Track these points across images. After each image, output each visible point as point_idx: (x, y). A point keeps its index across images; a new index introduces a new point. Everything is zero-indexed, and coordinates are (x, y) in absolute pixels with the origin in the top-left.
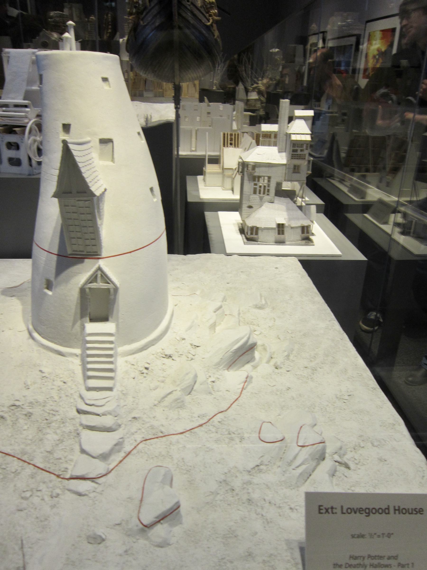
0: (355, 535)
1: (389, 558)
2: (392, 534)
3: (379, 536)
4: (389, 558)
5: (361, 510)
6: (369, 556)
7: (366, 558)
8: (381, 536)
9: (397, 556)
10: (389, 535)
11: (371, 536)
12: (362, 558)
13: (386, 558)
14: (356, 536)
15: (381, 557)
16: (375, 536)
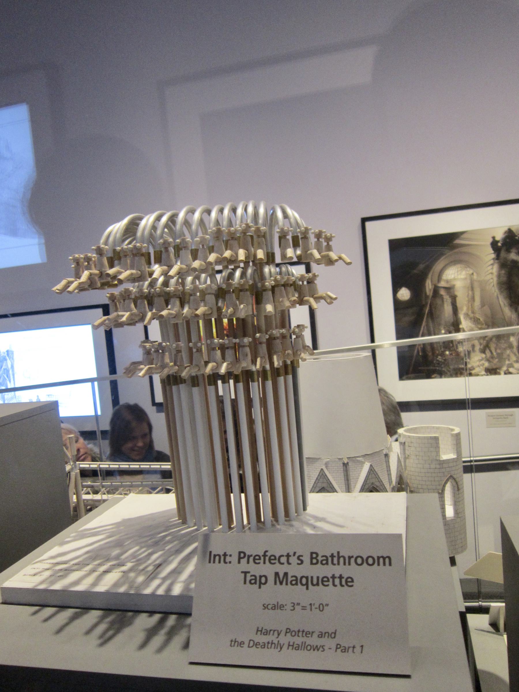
4: (321, 635)
6: (288, 631)
12: (276, 633)
13: (315, 635)
15: (308, 634)
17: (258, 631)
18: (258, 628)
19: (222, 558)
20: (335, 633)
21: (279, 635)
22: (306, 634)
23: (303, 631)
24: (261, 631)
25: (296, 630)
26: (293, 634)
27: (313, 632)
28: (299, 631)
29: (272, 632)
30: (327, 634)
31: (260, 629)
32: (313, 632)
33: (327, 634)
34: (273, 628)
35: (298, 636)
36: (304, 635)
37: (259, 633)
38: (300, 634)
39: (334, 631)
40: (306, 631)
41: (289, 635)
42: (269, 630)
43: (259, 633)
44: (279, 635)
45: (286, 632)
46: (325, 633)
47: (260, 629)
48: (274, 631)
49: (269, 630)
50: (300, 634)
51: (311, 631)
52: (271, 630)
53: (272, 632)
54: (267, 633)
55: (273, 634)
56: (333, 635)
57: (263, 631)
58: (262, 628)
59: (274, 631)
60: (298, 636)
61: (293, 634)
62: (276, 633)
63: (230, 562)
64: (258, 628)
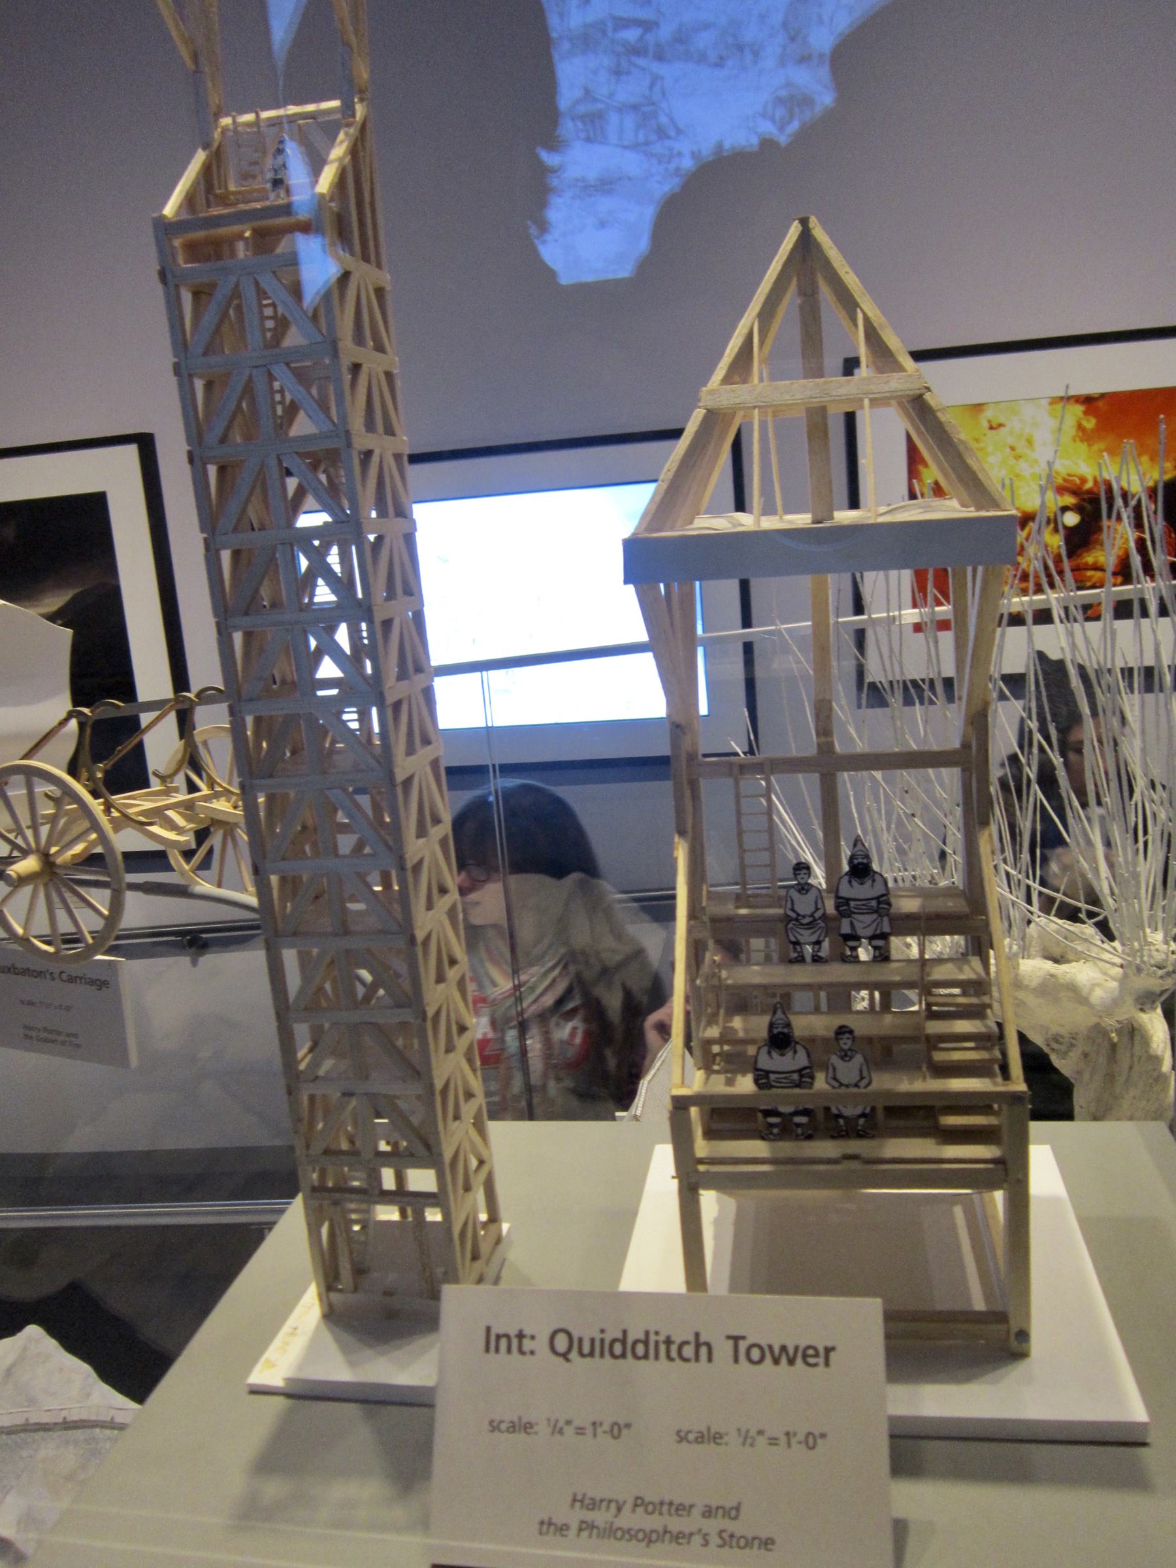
0: (689, 1432)
1: (708, 1513)
2: (823, 1436)
3: (773, 1441)
4: (708, 1513)
5: (811, 1352)
6: (639, 1502)
7: (627, 1508)
8: (783, 1440)
9: (737, 1509)
10: (811, 1441)
11: (747, 1439)
12: (613, 1506)
13: (696, 1512)
15: (681, 1509)
16: (761, 1441)
17: (575, 1500)
18: (575, 1495)
19: (515, 1342)
20: (737, 1509)
21: (619, 1509)
22: (677, 1510)
23: (671, 1504)
24: (582, 1501)
25: (656, 1500)
26: (650, 1508)
27: (691, 1506)
28: (662, 1503)
29: (604, 1504)
30: (720, 1512)
31: (579, 1497)
32: (691, 1506)
33: (720, 1512)
34: (608, 1495)
35: (661, 1514)
36: (673, 1511)
38: (665, 1508)
39: (735, 1504)
40: (677, 1501)
41: (640, 1510)
42: (598, 1499)
43: (578, 1504)
44: (619, 1509)
45: (636, 1505)
46: (718, 1508)
47: (579, 1497)
48: (610, 1501)
49: (598, 1499)
50: (665, 1508)
51: (687, 1503)
52: (602, 1501)
54: (594, 1505)
55: (608, 1508)
56: (733, 1513)
57: (587, 1501)
58: (584, 1495)
61: (650, 1508)
62: (613, 1506)
63: (532, 1353)
64: (575, 1495)
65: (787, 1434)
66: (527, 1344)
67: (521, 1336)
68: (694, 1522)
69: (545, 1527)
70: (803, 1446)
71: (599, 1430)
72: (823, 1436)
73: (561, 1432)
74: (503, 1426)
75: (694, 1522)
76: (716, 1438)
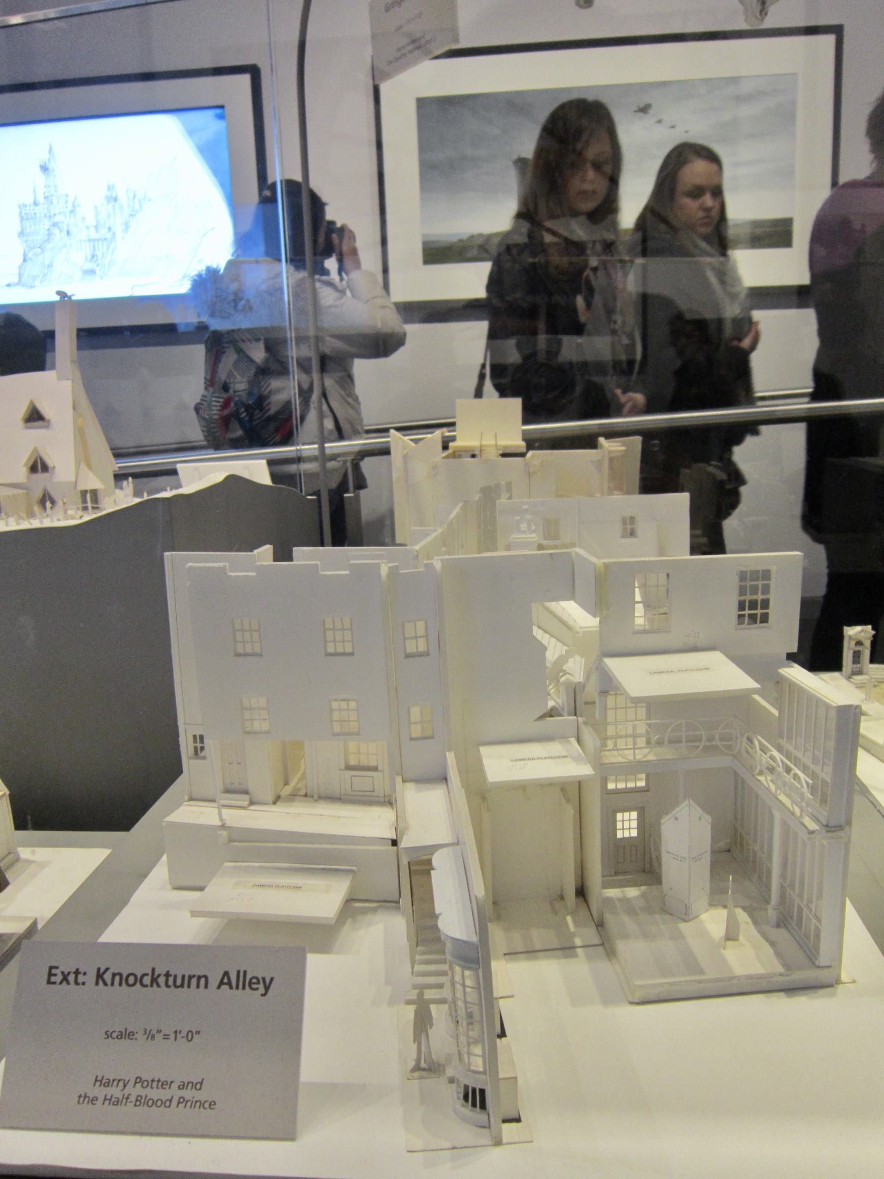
0: (114, 1031)
2: (198, 1033)
3: (166, 1037)
4: (182, 1086)
6: (139, 1080)
8: (172, 1036)
12: (121, 1084)
13: (175, 1086)
14: (114, 1035)
15: (164, 1084)
17: (96, 1080)
20: (201, 1084)
21: (125, 1086)
22: (162, 1084)
23: (159, 1081)
25: (149, 1080)
26: (145, 1084)
27: (171, 1082)
28: (153, 1081)
29: (116, 1082)
30: (190, 1085)
32: (171, 1082)
33: (190, 1085)
34: (119, 1077)
37: (98, 1083)
38: (155, 1084)
39: (200, 1081)
40: (162, 1079)
41: (139, 1085)
43: (98, 1083)
44: (125, 1086)
45: (136, 1083)
50: (155, 1084)
53: (116, 1082)
54: (108, 1084)
56: (198, 1086)
59: (119, 1081)
60: (152, 1087)
61: (145, 1084)
62: (121, 1084)
65: (176, 1032)
66: (81, 978)
67: (77, 972)
68: (174, 1092)
69: (82, 1099)
70: (185, 1039)
71: (179, 1036)
72: (198, 1033)
73: (153, 1037)
74: (114, 1035)
75: (174, 1092)
76: (129, 1035)
